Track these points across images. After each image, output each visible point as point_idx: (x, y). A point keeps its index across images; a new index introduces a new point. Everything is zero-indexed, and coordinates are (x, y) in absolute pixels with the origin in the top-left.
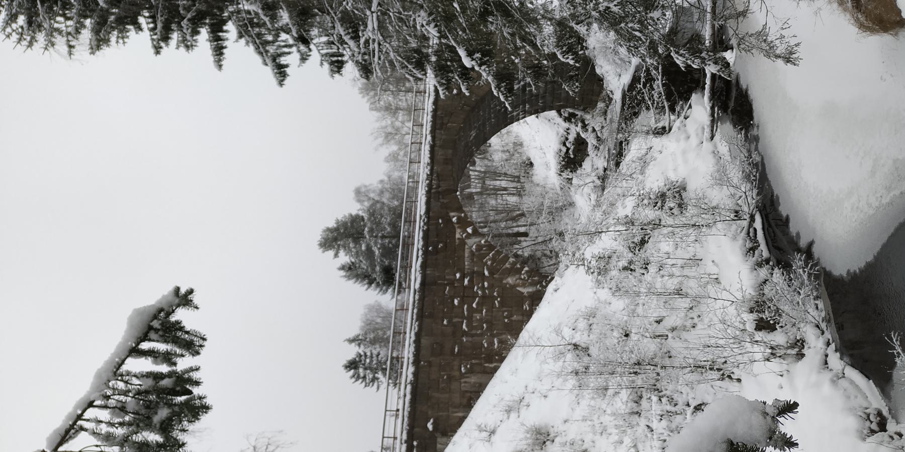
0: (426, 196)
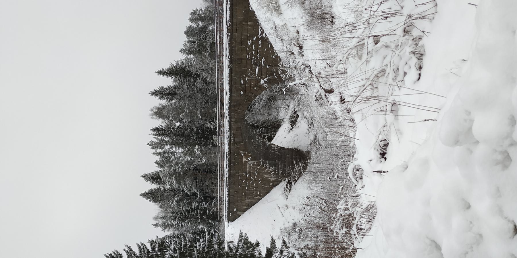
0: (229, 145)
